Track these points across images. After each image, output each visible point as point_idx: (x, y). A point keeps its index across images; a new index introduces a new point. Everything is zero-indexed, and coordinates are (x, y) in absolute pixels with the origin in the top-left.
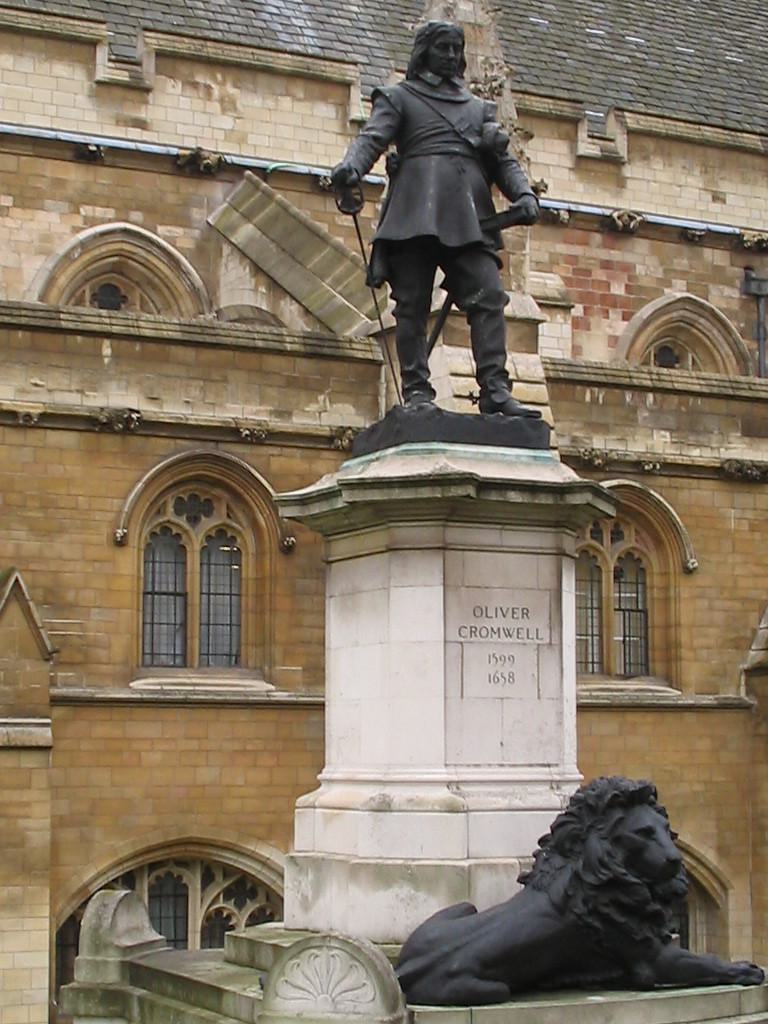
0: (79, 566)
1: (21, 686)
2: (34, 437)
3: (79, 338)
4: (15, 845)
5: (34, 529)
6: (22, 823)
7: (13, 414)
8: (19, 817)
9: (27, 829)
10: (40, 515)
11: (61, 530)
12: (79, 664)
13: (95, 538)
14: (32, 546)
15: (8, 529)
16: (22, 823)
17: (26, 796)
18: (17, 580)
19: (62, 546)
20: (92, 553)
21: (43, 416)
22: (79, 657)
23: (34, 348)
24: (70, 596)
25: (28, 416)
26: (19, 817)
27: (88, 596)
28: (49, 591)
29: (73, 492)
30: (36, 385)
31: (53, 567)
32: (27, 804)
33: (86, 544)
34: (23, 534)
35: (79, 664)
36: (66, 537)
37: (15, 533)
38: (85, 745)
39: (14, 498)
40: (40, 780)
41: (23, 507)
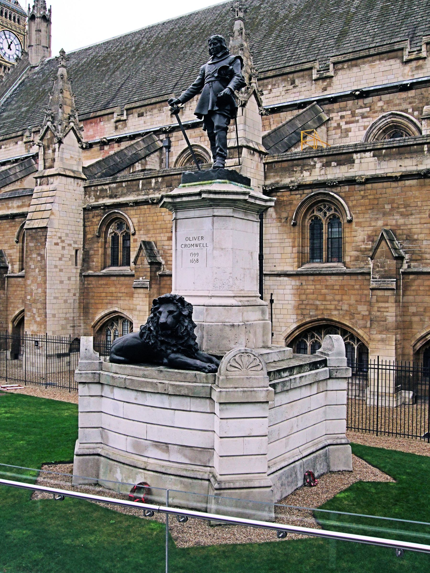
0: (419, 226)
1: (386, 268)
2: (401, 183)
3: (415, 147)
4: (383, 321)
5: (402, 214)
6: (385, 314)
7: (391, 177)
8: (384, 312)
9: (387, 316)
10: (404, 210)
11: (412, 214)
12: (419, 260)
13: (424, 216)
14: (401, 221)
15: (393, 216)
16: (385, 314)
17: (386, 305)
18: (382, 234)
19: (412, 220)
20: (423, 221)
21: (402, 176)
22: (419, 258)
23: (400, 154)
24: (416, 237)
25: (396, 177)
26: (384, 312)
27: (421, 236)
28: (408, 236)
29: (416, 200)
30: (400, 166)
31: (409, 227)
32: (388, 307)
33: (421, 218)
34: (398, 217)
35: (419, 260)
36: (414, 217)
37: (395, 217)
38: (421, 288)
39: (395, 205)
40: (392, 299)
41: (398, 208)
